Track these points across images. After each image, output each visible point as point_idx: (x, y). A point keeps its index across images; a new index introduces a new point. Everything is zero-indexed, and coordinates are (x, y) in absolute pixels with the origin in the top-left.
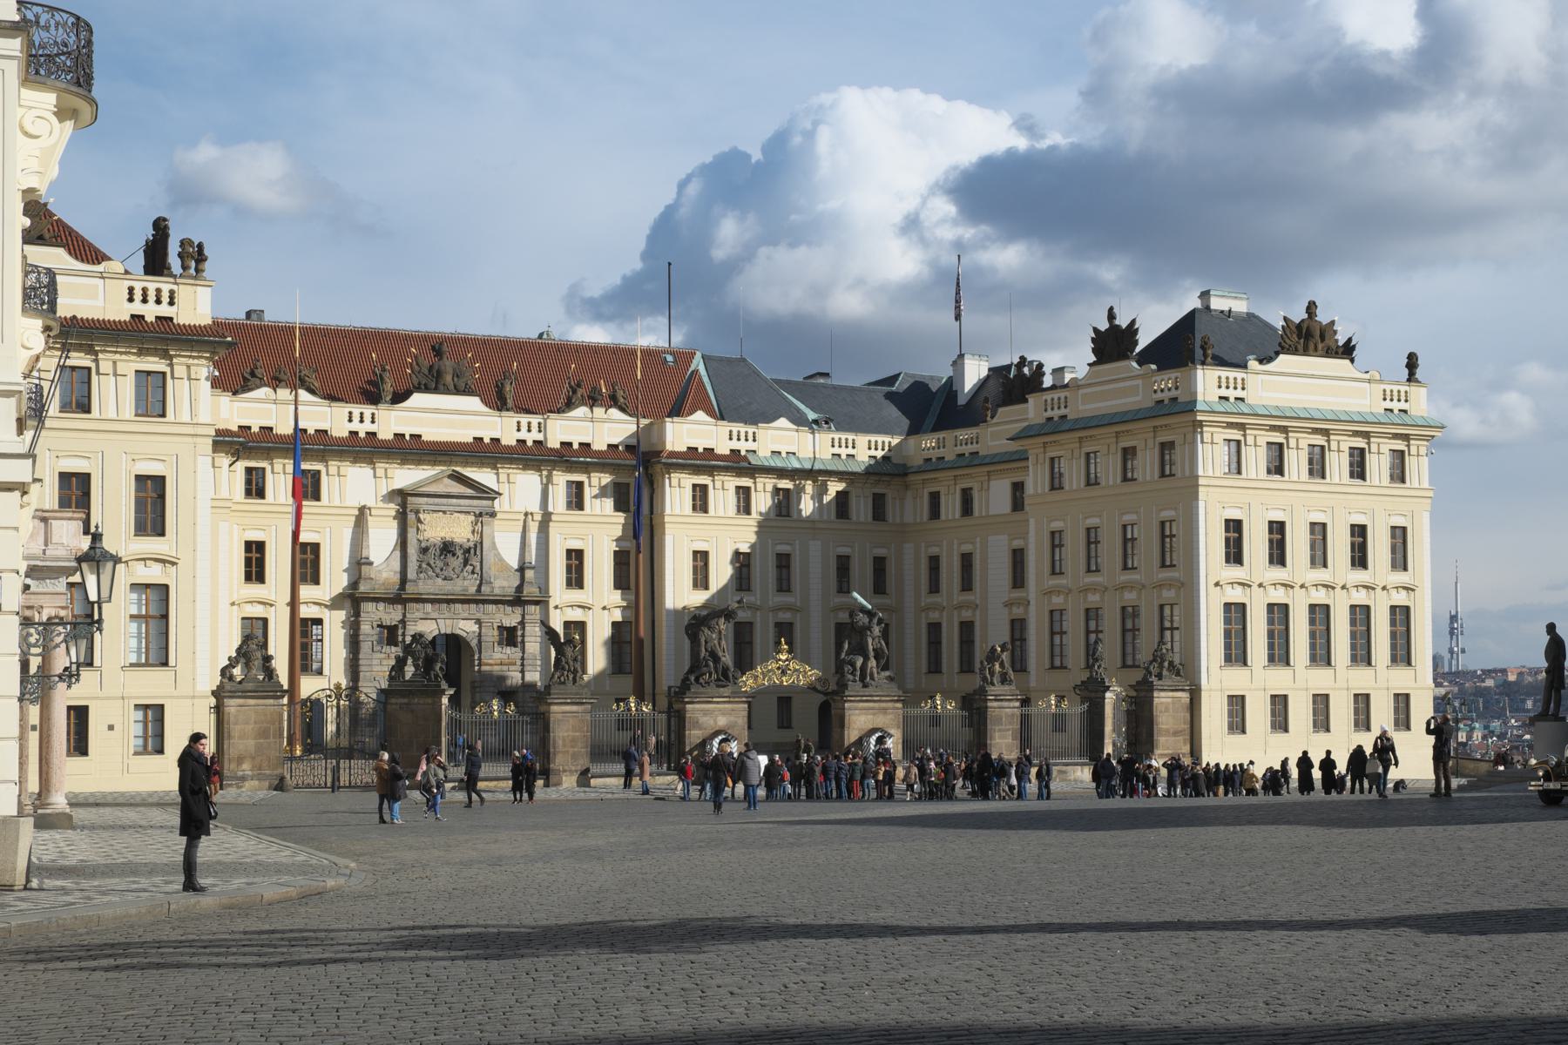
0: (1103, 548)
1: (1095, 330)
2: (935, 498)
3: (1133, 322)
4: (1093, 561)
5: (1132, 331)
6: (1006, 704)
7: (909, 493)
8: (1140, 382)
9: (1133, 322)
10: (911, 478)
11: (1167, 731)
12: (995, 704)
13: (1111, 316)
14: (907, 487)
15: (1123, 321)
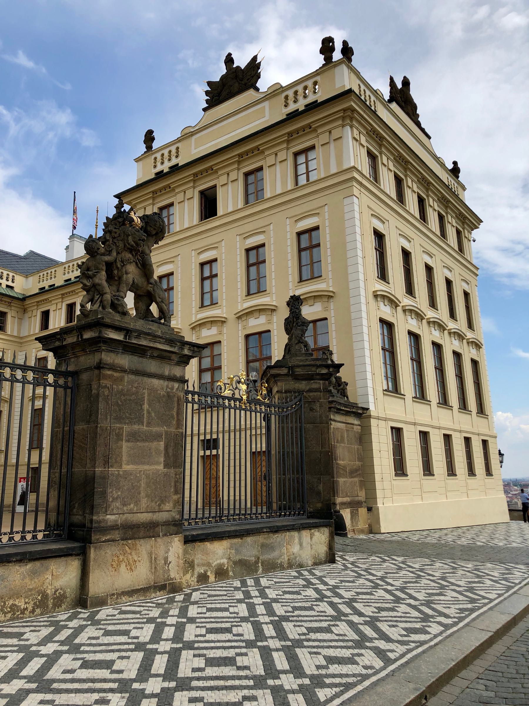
0: (221, 283)
1: (209, 83)
2: (46, 315)
3: (255, 58)
4: (207, 297)
5: (254, 66)
6: (152, 366)
7: (27, 315)
8: (266, 104)
9: (255, 58)
10: (28, 302)
11: (345, 467)
12: (124, 360)
13: (229, 60)
14: (25, 311)
15: (241, 61)
